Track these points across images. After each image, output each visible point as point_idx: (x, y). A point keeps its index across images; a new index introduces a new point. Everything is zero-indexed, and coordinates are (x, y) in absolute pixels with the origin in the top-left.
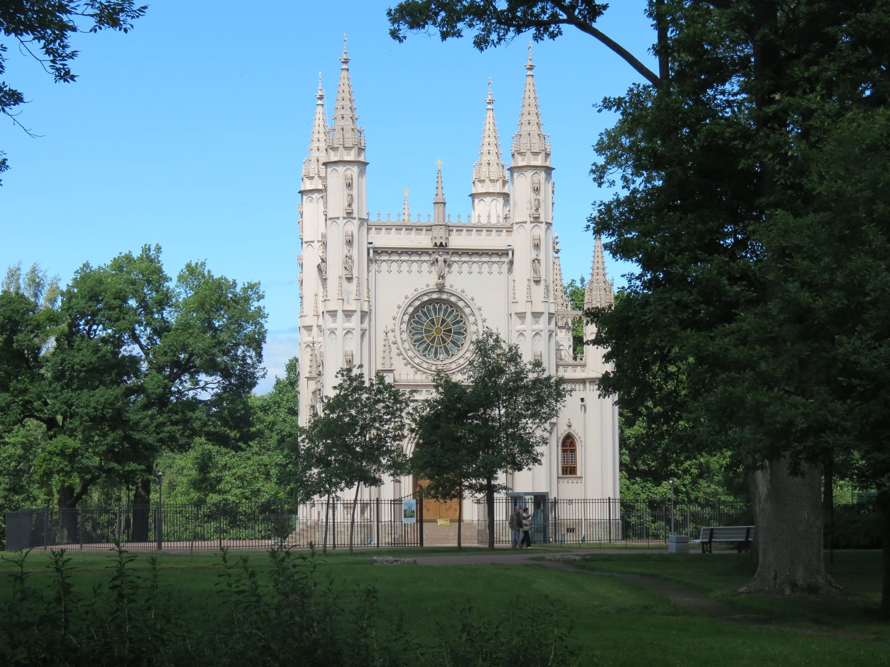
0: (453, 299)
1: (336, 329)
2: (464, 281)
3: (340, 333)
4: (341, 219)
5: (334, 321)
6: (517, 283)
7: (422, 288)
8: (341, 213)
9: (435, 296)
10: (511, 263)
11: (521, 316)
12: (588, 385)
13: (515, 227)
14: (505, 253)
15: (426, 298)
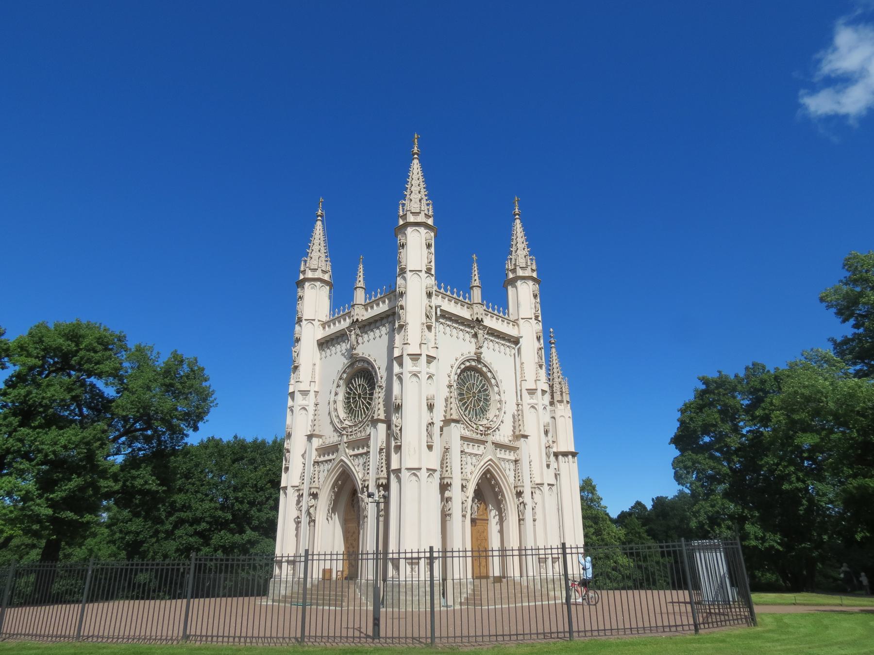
0: (484, 369)
1: (419, 372)
2: (496, 357)
3: (424, 376)
4: (423, 272)
5: (415, 365)
6: (525, 365)
7: (466, 356)
8: (424, 269)
9: (473, 364)
10: (519, 349)
11: (532, 392)
12: (560, 457)
13: (521, 322)
14: (516, 341)
15: (468, 364)
